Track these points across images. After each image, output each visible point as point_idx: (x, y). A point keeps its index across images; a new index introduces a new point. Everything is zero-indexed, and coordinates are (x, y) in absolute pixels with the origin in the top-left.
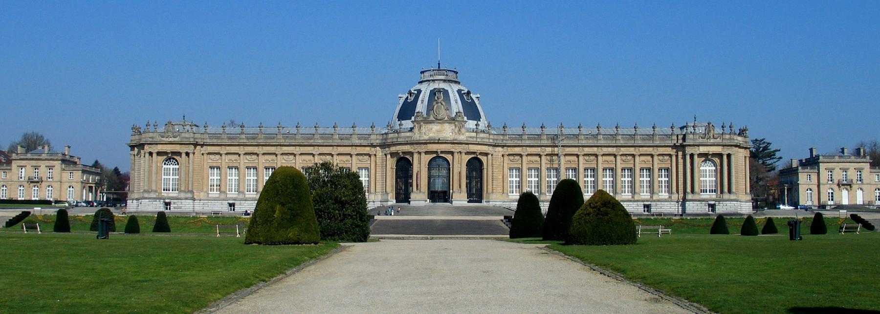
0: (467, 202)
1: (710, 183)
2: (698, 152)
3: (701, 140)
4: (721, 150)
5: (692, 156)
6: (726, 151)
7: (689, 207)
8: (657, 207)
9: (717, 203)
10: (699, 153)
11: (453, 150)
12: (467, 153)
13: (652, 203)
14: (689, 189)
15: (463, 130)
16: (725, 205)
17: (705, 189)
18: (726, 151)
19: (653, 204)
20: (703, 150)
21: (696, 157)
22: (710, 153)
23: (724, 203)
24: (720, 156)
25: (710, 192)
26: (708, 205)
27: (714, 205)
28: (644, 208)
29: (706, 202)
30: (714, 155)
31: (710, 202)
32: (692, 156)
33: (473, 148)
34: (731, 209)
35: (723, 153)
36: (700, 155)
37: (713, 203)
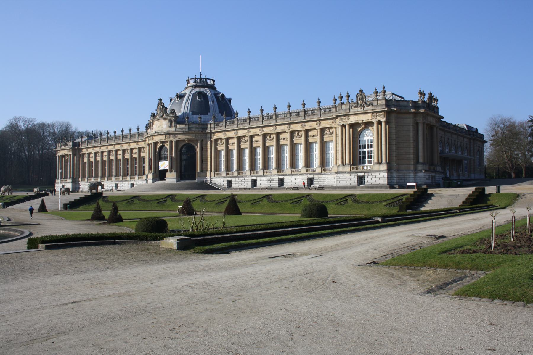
0: (175, 180)
1: (368, 153)
2: (350, 122)
7: (339, 180)
8: (319, 180)
9: (366, 174)
11: (167, 140)
12: (177, 142)
13: (315, 176)
15: (173, 124)
16: (374, 177)
17: (370, 160)
20: (353, 119)
23: (373, 174)
25: (368, 163)
26: (356, 177)
27: (364, 176)
29: (356, 174)
33: (179, 137)
34: (380, 181)
35: (373, 121)
37: (362, 174)
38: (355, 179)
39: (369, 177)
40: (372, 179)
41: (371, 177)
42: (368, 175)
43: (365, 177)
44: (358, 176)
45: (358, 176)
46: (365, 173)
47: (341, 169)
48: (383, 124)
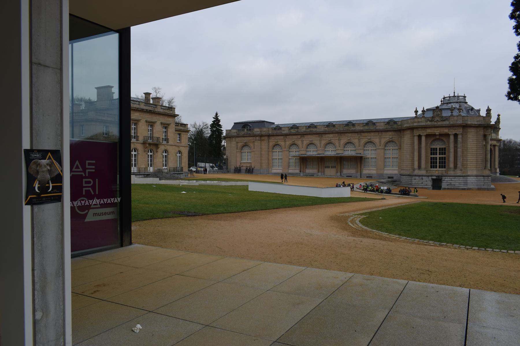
3: (429, 123)
4: (447, 131)
5: (420, 137)
6: (452, 132)
20: (429, 131)
24: (447, 135)
26: (431, 179)
30: (440, 135)
31: (433, 177)
32: (420, 137)
35: (450, 133)
36: (427, 136)
47: (417, 172)
48: (460, 137)
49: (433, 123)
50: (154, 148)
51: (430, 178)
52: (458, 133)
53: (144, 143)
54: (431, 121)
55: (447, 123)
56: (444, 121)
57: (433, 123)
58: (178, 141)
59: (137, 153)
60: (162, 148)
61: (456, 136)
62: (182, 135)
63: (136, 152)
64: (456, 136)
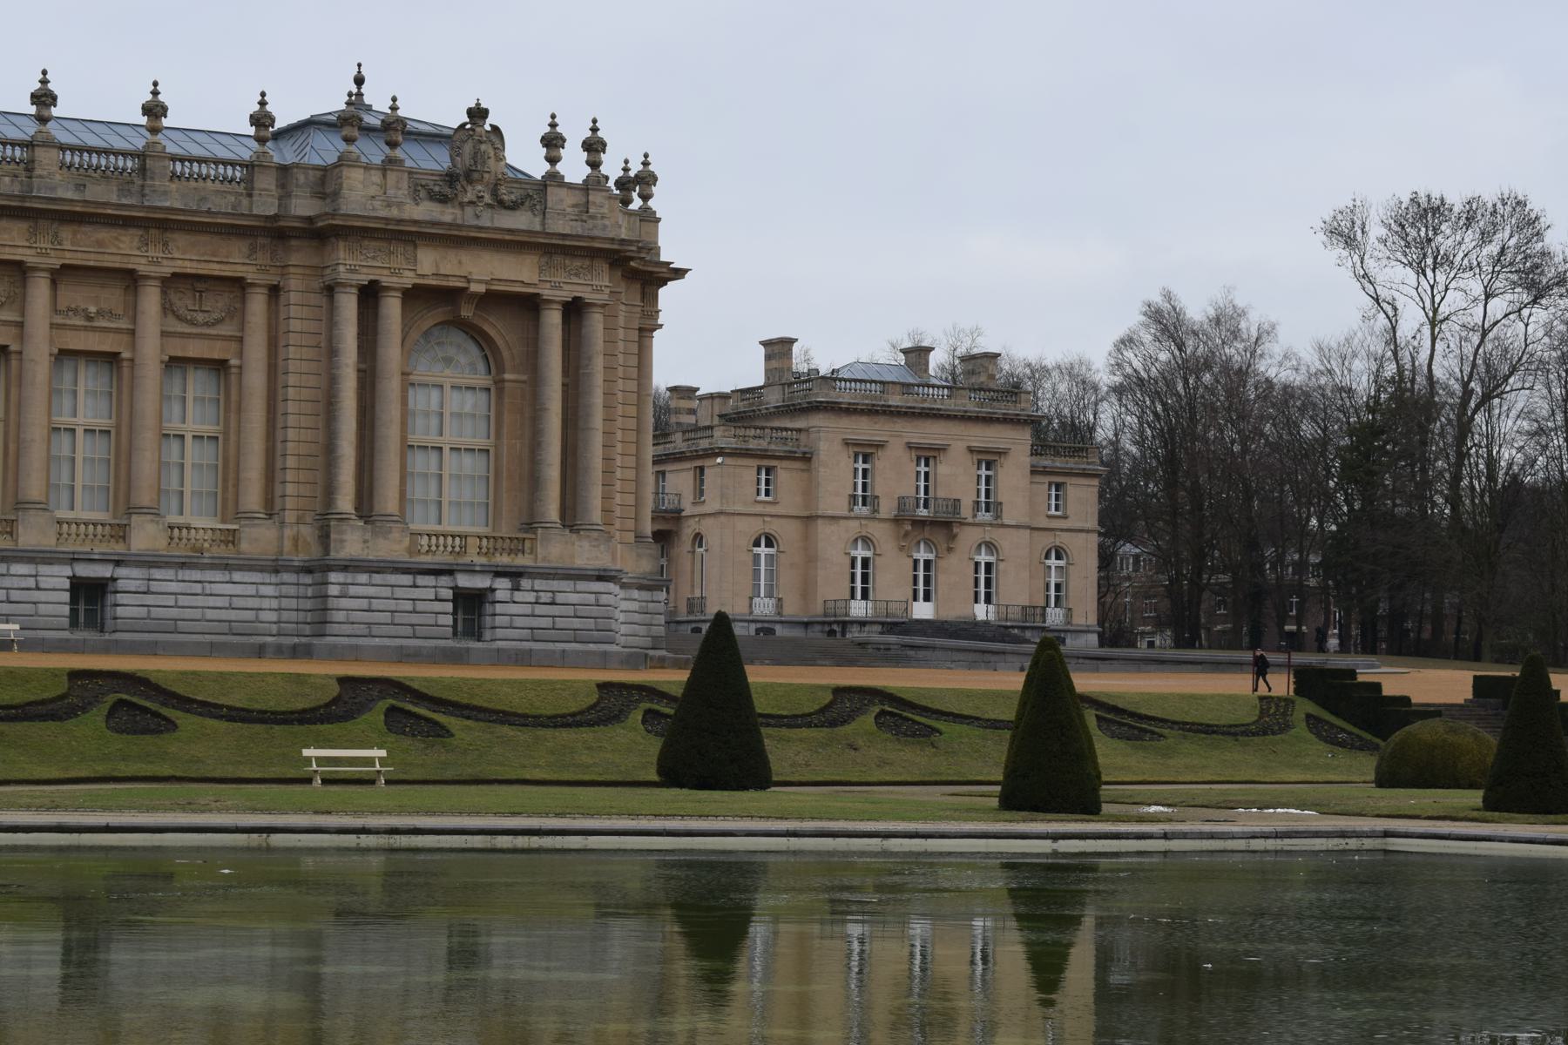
2: (408, 280)
3: (425, 211)
5: (370, 294)
6: (560, 285)
7: (344, 603)
9: (503, 584)
10: (416, 286)
13: (122, 572)
14: (345, 502)
16: (545, 597)
18: (560, 285)
19: (129, 577)
20: (430, 265)
21: (392, 308)
22: (475, 288)
23: (539, 584)
24: (528, 305)
26: (449, 594)
28: (74, 601)
29: (444, 580)
30: (496, 300)
31: (464, 581)
32: (370, 294)
35: (546, 292)
36: (417, 296)
37: (481, 582)
38: (438, 606)
39: (518, 596)
40: (539, 610)
41: (531, 597)
42: (516, 588)
43: (499, 595)
44: (455, 589)
45: (455, 589)
46: (498, 574)
49: (447, 214)
50: (939, 537)
51: (444, 584)
52: (588, 295)
53: (897, 521)
54: (443, 199)
55: (521, 221)
56: (514, 207)
57: (447, 214)
58: (762, 497)
59: (874, 554)
60: (968, 538)
61: (574, 310)
62: (779, 470)
63: (772, 546)
64: (574, 310)
